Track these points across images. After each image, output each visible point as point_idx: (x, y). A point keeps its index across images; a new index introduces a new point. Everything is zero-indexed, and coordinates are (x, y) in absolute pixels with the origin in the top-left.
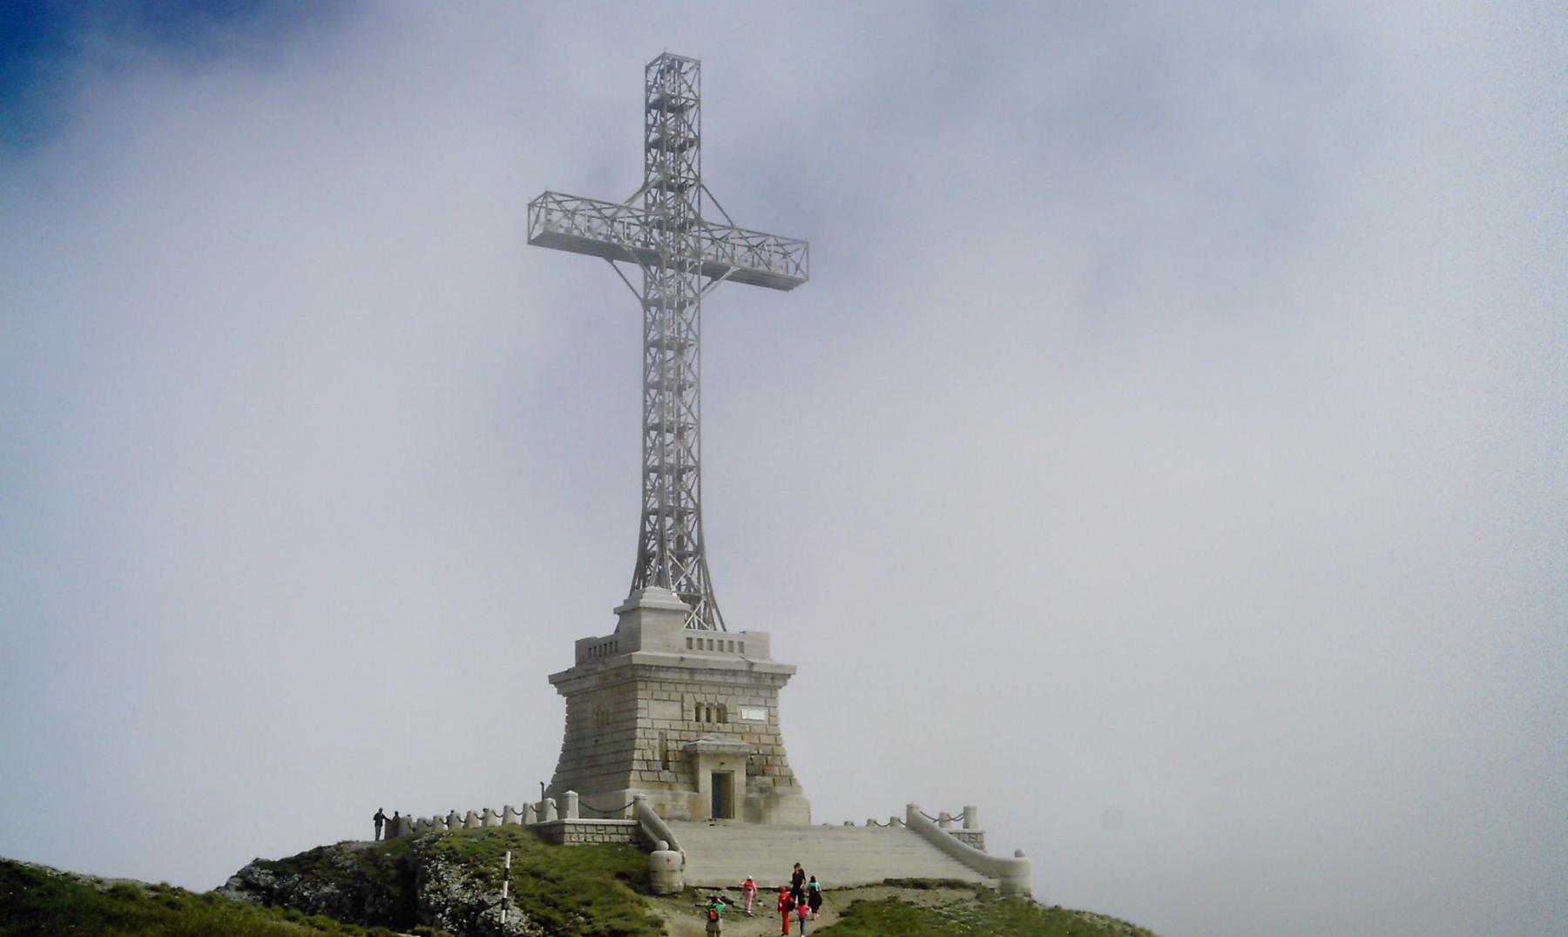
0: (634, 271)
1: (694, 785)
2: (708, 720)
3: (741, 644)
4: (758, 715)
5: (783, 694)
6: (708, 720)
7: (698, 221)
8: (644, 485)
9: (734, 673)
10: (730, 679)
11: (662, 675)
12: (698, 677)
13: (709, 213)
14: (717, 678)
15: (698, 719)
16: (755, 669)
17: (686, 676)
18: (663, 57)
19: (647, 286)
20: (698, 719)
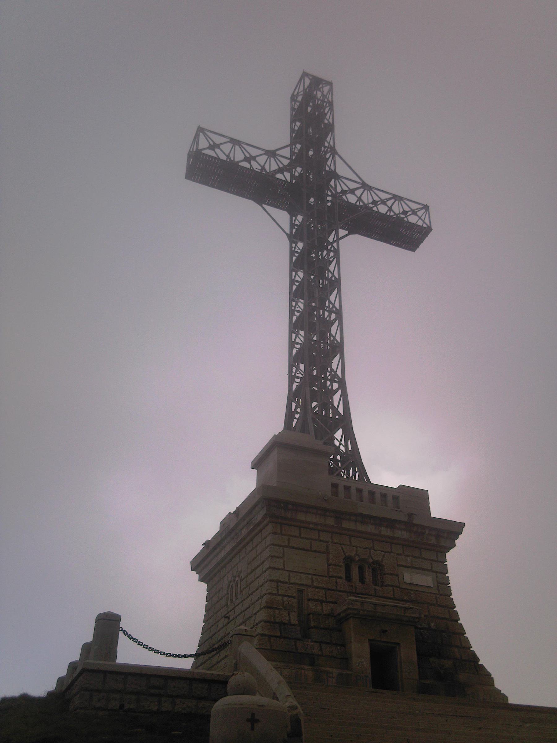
0: (283, 217)
1: (345, 660)
2: (362, 580)
3: (396, 498)
4: (424, 580)
5: (451, 557)
6: (362, 580)
7: (334, 175)
8: (290, 371)
9: (391, 523)
10: (385, 531)
11: (301, 517)
12: (346, 525)
13: (341, 169)
14: (370, 529)
15: (348, 578)
16: (415, 522)
17: (331, 521)
18: (305, 74)
19: (292, 225)
20: (348, 578)
